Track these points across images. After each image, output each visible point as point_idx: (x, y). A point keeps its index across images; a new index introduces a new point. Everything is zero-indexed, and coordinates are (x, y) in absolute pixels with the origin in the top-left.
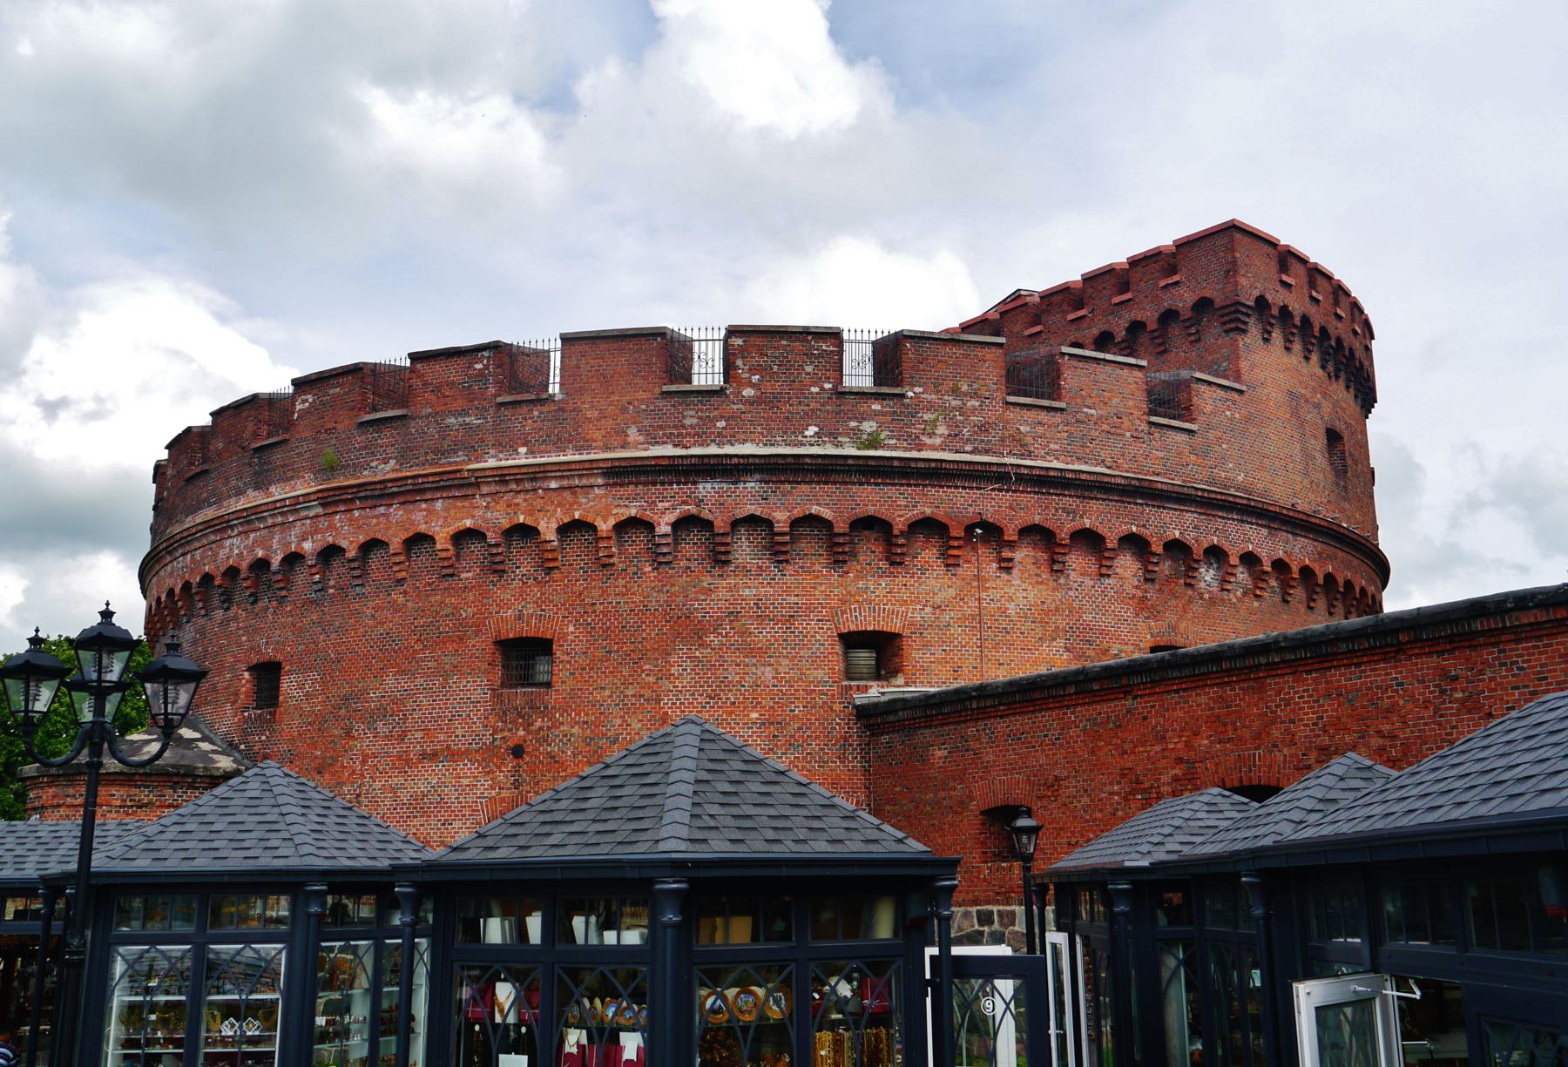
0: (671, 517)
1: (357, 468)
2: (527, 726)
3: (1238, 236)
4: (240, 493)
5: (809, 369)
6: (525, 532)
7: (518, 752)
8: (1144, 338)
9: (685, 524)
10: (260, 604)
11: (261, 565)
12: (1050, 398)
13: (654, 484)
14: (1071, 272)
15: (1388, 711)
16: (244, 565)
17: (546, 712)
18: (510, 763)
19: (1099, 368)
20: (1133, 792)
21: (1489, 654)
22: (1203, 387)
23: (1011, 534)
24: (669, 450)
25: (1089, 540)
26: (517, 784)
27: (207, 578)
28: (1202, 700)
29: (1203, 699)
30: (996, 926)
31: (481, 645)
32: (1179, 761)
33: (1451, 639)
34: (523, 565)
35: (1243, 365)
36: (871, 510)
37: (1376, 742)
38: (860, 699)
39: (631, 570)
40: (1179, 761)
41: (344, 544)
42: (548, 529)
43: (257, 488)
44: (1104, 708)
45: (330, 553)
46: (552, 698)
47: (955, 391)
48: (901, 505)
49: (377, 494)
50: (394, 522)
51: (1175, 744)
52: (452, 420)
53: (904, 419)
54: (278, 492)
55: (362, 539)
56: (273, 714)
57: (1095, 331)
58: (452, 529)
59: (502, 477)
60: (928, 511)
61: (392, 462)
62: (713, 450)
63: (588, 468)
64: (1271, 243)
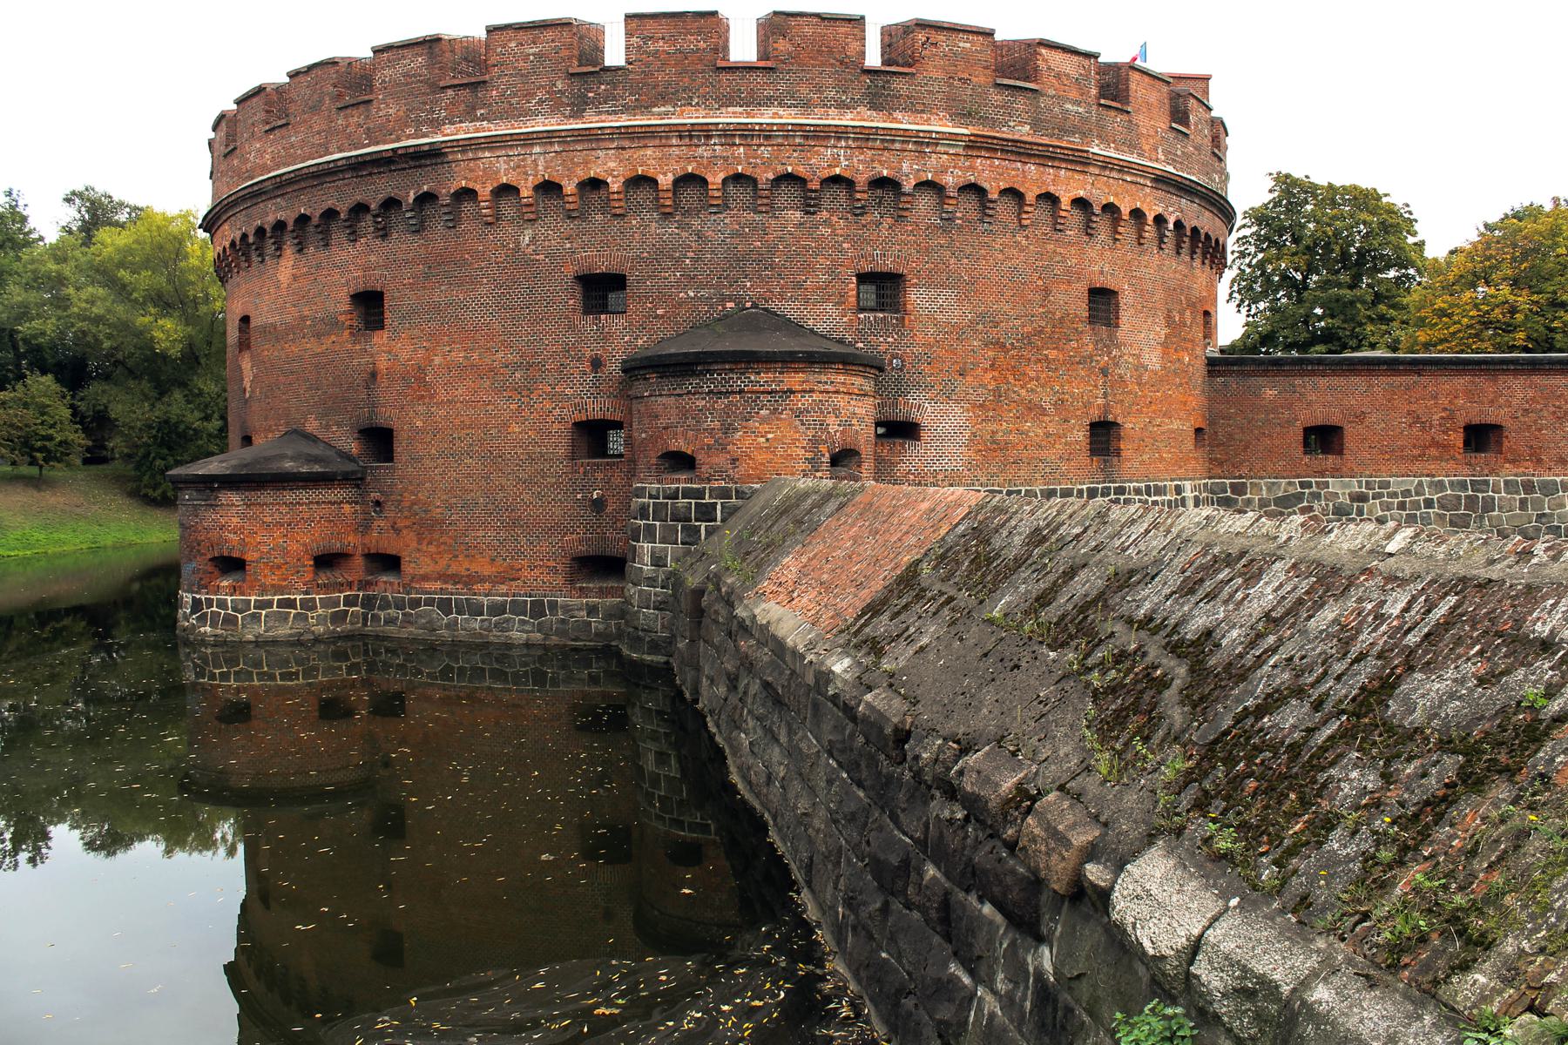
1: (993, 123)
4: (842, 106)
7: (1104, 372)
10: (868, 218)
16: (861, 179)
17: (1118, 347)
26: (1105, 395)
28: (1461, 382)
30: (1314, 489)
31: (1081, 289)
43: (874, 106)
46: (1120, 334)
49: (1019, 151)
50: (1032, 178)
51: (1444, 401)
52: (1069, 106)
54: (904, 122)
55: (1003, 185)
56: (1111, 337)
59: (1107, 165)
61: (1027, 127)
63: (1142, 171)
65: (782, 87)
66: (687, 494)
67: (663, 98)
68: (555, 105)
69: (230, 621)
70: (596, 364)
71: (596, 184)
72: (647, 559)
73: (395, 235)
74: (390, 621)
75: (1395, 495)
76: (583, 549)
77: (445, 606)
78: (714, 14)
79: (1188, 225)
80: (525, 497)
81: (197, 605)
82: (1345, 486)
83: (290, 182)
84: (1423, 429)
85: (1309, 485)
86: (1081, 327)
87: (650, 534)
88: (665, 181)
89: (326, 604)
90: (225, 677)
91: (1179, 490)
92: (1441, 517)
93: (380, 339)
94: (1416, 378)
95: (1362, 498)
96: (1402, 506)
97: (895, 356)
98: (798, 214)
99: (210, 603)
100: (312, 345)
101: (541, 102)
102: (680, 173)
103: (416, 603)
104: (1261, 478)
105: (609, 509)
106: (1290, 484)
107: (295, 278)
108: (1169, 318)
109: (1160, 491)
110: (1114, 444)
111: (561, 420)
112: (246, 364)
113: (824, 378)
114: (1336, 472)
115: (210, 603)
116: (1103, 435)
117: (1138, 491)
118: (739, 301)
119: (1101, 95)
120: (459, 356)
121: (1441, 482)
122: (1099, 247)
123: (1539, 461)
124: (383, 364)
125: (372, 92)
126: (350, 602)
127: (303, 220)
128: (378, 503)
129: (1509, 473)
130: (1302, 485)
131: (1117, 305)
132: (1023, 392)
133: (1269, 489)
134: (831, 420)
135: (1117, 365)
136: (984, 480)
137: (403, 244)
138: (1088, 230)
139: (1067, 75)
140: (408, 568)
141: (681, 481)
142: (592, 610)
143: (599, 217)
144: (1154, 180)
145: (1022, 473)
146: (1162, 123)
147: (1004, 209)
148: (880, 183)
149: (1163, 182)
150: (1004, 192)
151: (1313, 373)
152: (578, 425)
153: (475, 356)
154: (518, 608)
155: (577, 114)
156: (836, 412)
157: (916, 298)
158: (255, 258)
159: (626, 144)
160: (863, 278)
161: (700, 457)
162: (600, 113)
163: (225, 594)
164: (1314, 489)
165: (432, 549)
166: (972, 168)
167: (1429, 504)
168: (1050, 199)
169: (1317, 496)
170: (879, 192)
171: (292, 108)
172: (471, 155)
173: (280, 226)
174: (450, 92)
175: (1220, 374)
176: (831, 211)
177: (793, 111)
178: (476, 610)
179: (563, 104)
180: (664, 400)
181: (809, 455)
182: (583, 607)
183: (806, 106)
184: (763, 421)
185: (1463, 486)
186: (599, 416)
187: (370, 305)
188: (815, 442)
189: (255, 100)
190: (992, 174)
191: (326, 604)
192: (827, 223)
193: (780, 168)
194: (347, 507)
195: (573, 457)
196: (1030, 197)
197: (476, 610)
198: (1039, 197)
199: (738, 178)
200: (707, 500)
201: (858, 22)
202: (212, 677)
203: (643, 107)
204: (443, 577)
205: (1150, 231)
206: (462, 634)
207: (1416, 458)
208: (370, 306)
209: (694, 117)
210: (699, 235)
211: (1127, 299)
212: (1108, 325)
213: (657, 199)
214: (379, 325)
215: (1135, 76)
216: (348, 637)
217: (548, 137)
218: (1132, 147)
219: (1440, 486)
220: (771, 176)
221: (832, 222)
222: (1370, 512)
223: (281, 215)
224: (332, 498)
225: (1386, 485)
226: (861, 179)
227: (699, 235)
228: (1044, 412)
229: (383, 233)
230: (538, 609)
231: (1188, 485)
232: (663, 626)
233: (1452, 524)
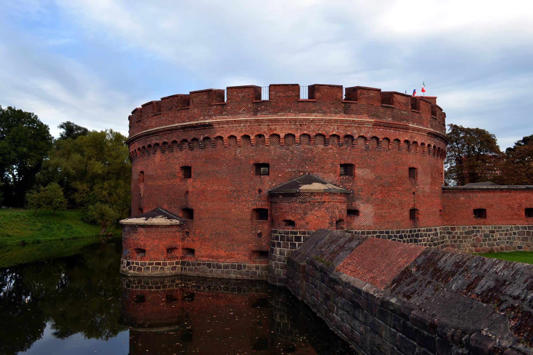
1: (381, 118)
4: (336, 113)
10: (343, 147)
24: (432, 130)
26: (414, 201)
28: (524, 194)
31: (406, 168)
50: (392, 134)
52: (402, 112)
59: (414, 129)
65: (318, 107)
66: (292, 233)
67: (282, 110)
68: (248, 111)
69: (140, 269)
70: (260, 191)
71: (260, 136)
72: (278, 253)
73: (195, 149)
74: (191, 270)
75: (503, 231)
76: (255, 249)
77: (209, 265)
78: (297, 85)
79: (437, 147)
80: (237, 232)
81: (128, 264)
82: (487, 228)
83: (162, 132)
85: (476, 228)
87: (279, 245)
88: (282, 135)
89: (170, 264)
90: (137, 287)
91: (436, 230)
92: (519, 238)
93: (190, 181)
94: (509, 193)
95: (493, 232)
96: (506, 235)
97: (351, 190)
98: (322, 146)
99: (133, 263)
100: (167, 182)
101: (244, 110)
102: (287, 133)
103: (199, 264)
105: (263, 236)
106: (469, 227)
107: (161, 161)
108: (432, 176)
109: (430, 230)
110: (416, 216)
111: (248, 208)
112: (142, 186)
113: (334, 198)
115: (133, 263)
116: (413, 213)
117: (424, 231)
118: (304, 172)
119: (412, 108)
120: (216, 187)
121: (518, 227)
124: (190, 189)
125: (189, 105)
126: (177, 263)
127: (165, 143)
128: (187, 232)
130: (473, 228)
131: (417, 173)
133: (463, 229)
134: (336, 211)
135: (417, 191)
136: (378, 228)
137: (197, 152)
138: (409, 149)
139: (402, 103)
140: (197, 253)
141: (290, 229)
142: (257, 268)
143: (261, 146)
144: (428, 134)
146: (429, 116)
147: (384, 144)
148: (347, 136)
149: (430, 134)
150: (384, 139)
152: (254, 210)
153: (221, 187)
154: (233, 267)
155: (255, 114)
156: (338, 208)
157: (358, 172)
158: (146, 153)
159: (270, 124)
160: (341, 165)
161: (296, 222)
162: (262, 114)
163: (138, 261)
164: (477, 229)
165: (205, 247)
167: (515, 234)
168: (398, 140)
169: (478, 231)
170: (347, 139)
171: (162, 109)
172: (221, 126)
173: (157, 144)
174: (215, 107)
175: (446, 192)
177: (321, 115)
178: (219, 267)
179: (251, 111)
180: (284, 204)
181: (330, 222)
182: (254, 267)
183: (325, 113)
184: (317, 210)
185: (525, 228)
186: (260, 207)
187: (187, 171)
188: (331, 217)
189: (149, 106)
190: (380, 133)
191: (170, 264)
192: (331, 149)
193: (317, 132)
194: (177, 234)
195: (251, 220)
196: (392, 140)
197: (219, 267)
199: (304, 135)
200: (298, 235)
201: (341, 87)
202: (132, 287)
203: (276, 113)
204: (209, 256)
205: (426, 149)
206: (215, 275)
207: (510, 219)
208: (187, 171)
209: (291, 117)
210: (292, 152)
211: (420, 170)
212: (414, 179)
213: (279, 141)
214: (190, 177)
215: (421, 102)
216: (176, 276)
217: (246, 121)
218: (421, 123)
219: (518, 228)
220: (314, 134)
221: (332, 149)
222: (496, 236)
223: (157, 142)
224: (173, 230)
225: (500, 228)
226: (342, 136)
227: (292, 152)
229: (192, 149)
230: (240, 267)
231: (438, 228)
232: (283, 274)
233: (522, 240)
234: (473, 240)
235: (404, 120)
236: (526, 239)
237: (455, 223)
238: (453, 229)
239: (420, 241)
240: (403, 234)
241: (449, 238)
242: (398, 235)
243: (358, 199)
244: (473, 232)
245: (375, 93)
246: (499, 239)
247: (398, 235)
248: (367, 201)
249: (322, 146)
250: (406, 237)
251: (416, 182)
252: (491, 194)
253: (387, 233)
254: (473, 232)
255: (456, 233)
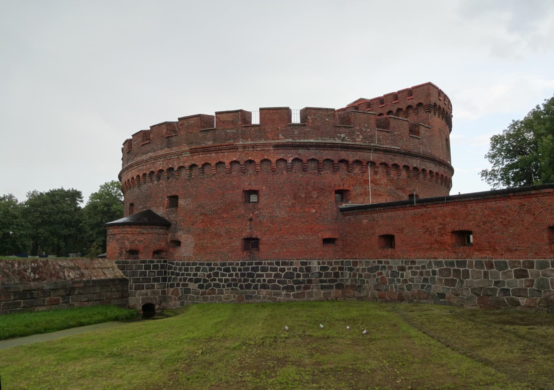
0: (291, 159)
2: (253, 213)
3: (431, 86)
4: (162, 149)
5: (327, 119)
6: (251, 161)
7: (251, 220)
8: (401, 113)
9: (295, 160)
10: (170, 180)
11: (171, 169)
12: (348, 124)
13: (287, 149)
14: (380, 94)
15: (504, 213)
16: (165, 169)
17: (258, 210)
18: (248, 223)
19: (398, 121)
20: (426, 232)
21: (535, 199)
22: (422, 127)
23: (377, 165)
25: (396, 166)
26: (251, 228)
27: (152, 172)
29: (448, 209)
31: (240, 191)
32: (440, 224)
33: (524, 195)
34: (251, 169)
35: (430, 121)
36: (343, 158)
37: (500, 220)
38: (340, 207)
39: (280, 172)
40: (440, 224)
41: (197, 164)
42: (257, 161)
43: (168, 147)
44: (418, 210)
45: (193, 166)
47: (364, 126)
48: (351, 156)
49: (206, 150)
50: (213, 158)
53: (351, 134)
54: (175, 150)
55: (203, 163)
57: (388, 110)
58: (230, 161)
59: (244, 147)
60: (358, 158)
61: (211, 142)
62: (302, 141)
64: (437, 88)
75: (418, 268)
84: (430, 235)
85: (380, 262)
86: (238, 205)
94: (425, 209)
95: (402, 269)
104: (363, 259)
108: (296, 197)
113: (123, 230)
114: (392, 257)
116: (251, 243)
122: (249, 176)
123: (495, 250)
129: (476, 257)
132: (213, 229)
133: (366, 265)
139: (228, 121)
145: (212, 257)
151: (380, 211)
157: (181, 202)
164: (383, 264)
166: (193, 160)
169: (384, 268)
176: (163, 180)
185: (452, 264)
188: (121, 248)
190: (199, 159)
198: (217, 164)
226: (165, 169)
228: (221, 236)
234: (377, 280)
235: (230, 140)
236: (451, 283)
237: (357, 256)
238: (355, 264)
239: (262, 276)
240: (231, 267)
241: (350, 276)
242: (223, 268)
243: (180, 229)
244: (377, 268)
245: (194, 120)
246: (412, 280)
247: (223, 268)
248: (188, 232)
249: (156, 182)
250: (234, 269)
251: (177, 210)
252: (400, 213)
253: (209, 264)
254: (377, 268)
255: (358, 270)
